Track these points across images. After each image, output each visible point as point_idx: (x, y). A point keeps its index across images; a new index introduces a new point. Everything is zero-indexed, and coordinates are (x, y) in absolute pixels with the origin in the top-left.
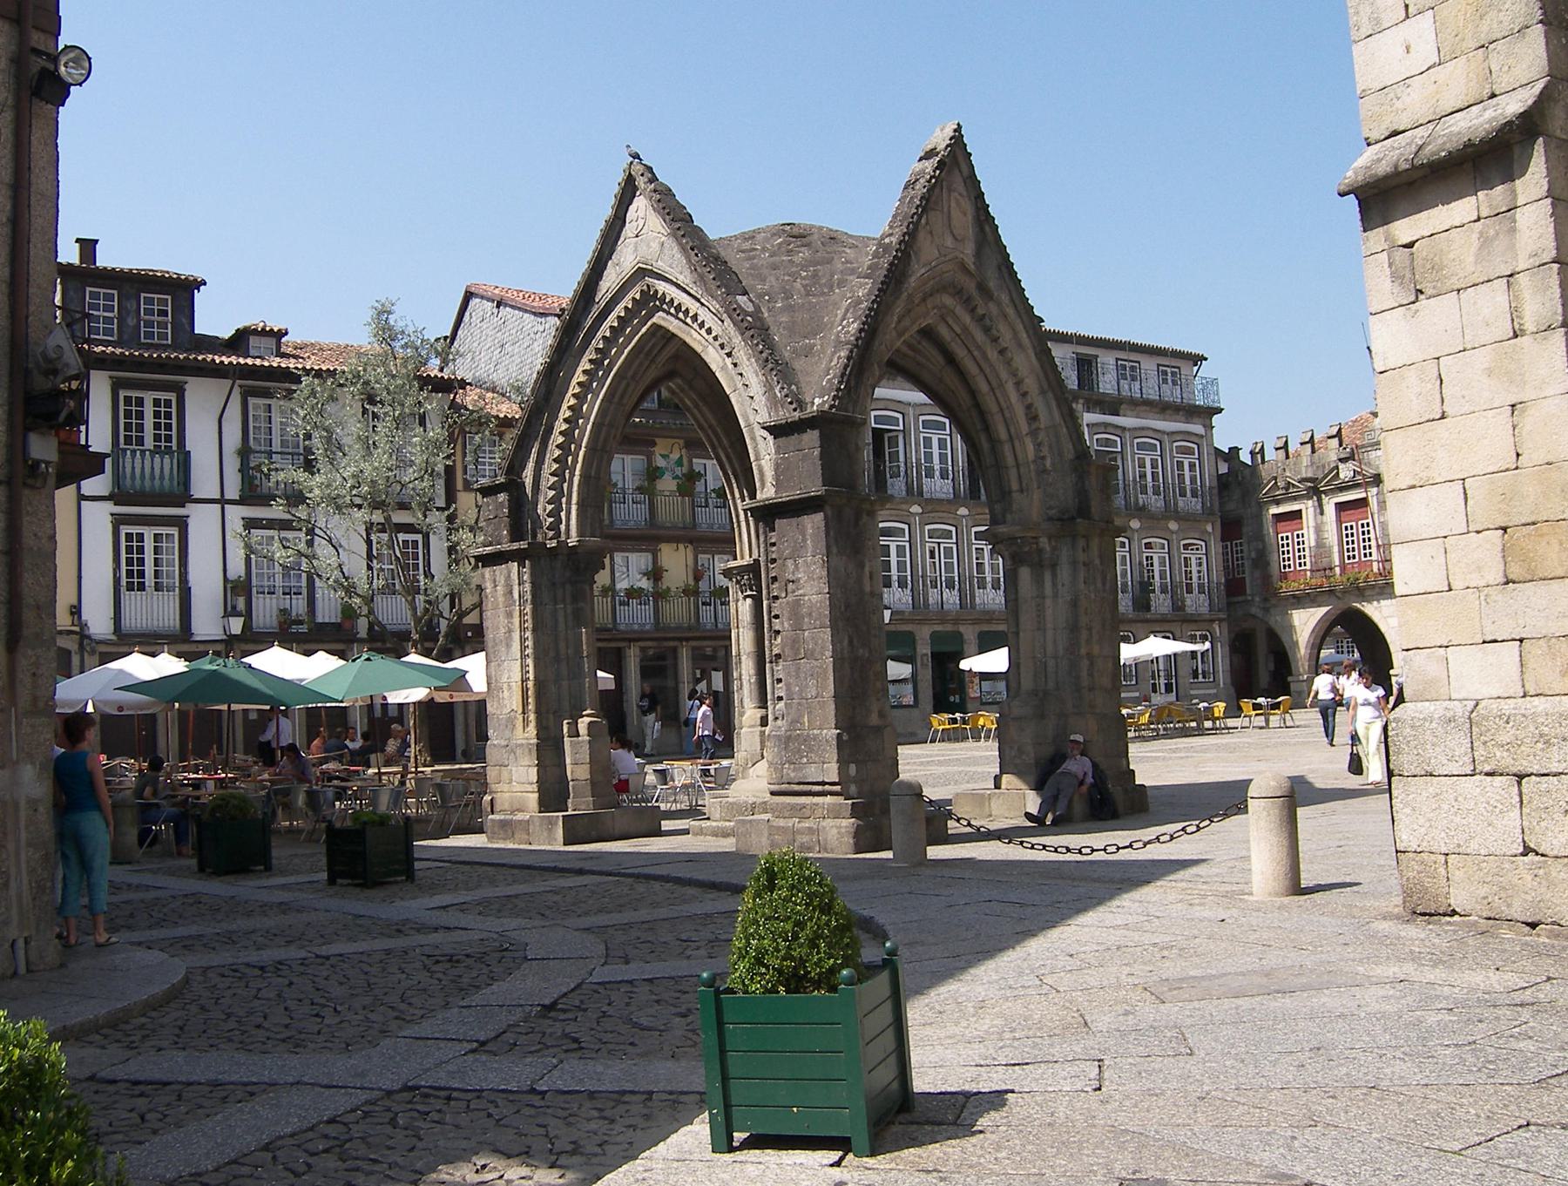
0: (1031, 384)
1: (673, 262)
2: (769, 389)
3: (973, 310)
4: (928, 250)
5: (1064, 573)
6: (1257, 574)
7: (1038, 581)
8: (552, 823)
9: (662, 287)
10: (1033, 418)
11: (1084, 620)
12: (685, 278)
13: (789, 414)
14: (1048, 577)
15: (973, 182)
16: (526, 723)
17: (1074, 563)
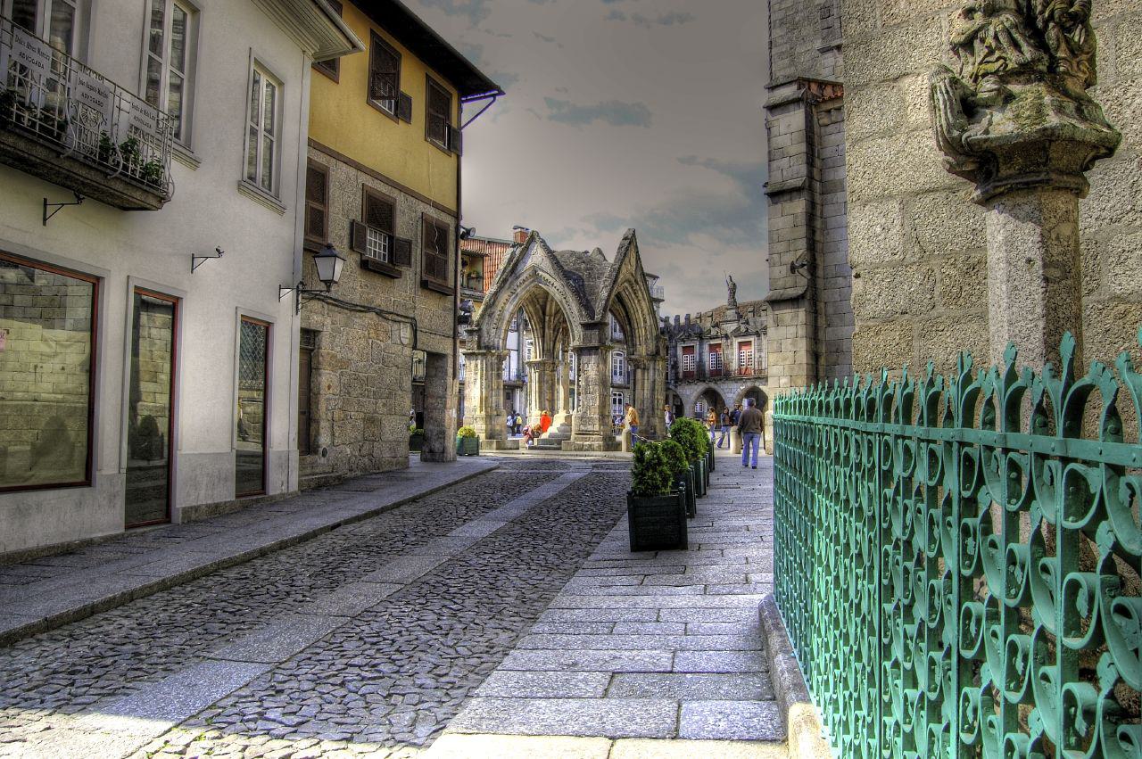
0: (646, 311)
1: (546, 265)
2: (580, 311)
3: (632, 288)
4: (624, 270)
5: (651, 372)
6: (673, 371)
7: (643, 374)
8: (492, 443)
9: (541, 273)
10: (645, 322)
11: (656, 387)
12: (552, 272)
13: (587, 321)
14: (646, 374)
15: (637, 247)
16: (481, 410)
17: (654, 369)
